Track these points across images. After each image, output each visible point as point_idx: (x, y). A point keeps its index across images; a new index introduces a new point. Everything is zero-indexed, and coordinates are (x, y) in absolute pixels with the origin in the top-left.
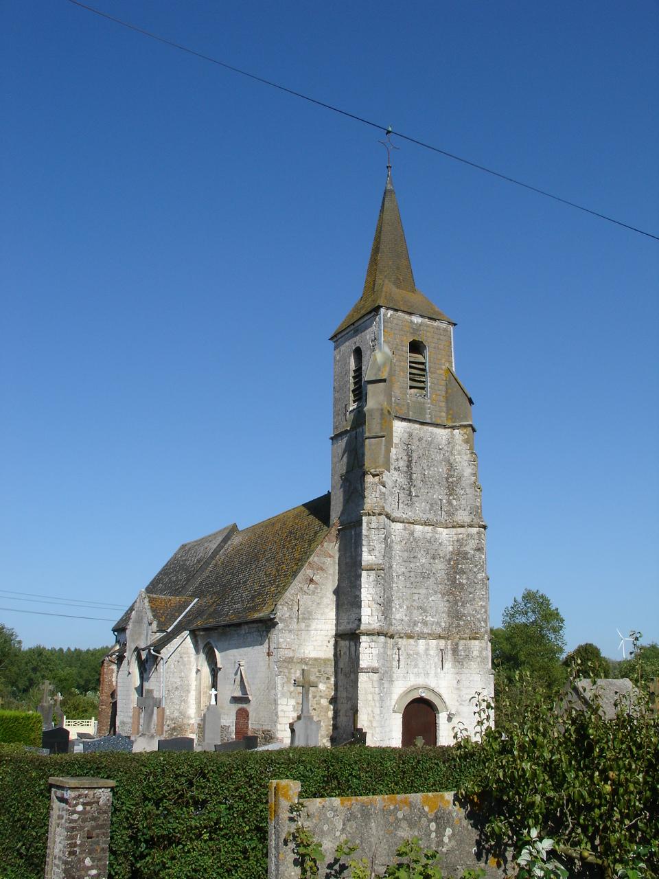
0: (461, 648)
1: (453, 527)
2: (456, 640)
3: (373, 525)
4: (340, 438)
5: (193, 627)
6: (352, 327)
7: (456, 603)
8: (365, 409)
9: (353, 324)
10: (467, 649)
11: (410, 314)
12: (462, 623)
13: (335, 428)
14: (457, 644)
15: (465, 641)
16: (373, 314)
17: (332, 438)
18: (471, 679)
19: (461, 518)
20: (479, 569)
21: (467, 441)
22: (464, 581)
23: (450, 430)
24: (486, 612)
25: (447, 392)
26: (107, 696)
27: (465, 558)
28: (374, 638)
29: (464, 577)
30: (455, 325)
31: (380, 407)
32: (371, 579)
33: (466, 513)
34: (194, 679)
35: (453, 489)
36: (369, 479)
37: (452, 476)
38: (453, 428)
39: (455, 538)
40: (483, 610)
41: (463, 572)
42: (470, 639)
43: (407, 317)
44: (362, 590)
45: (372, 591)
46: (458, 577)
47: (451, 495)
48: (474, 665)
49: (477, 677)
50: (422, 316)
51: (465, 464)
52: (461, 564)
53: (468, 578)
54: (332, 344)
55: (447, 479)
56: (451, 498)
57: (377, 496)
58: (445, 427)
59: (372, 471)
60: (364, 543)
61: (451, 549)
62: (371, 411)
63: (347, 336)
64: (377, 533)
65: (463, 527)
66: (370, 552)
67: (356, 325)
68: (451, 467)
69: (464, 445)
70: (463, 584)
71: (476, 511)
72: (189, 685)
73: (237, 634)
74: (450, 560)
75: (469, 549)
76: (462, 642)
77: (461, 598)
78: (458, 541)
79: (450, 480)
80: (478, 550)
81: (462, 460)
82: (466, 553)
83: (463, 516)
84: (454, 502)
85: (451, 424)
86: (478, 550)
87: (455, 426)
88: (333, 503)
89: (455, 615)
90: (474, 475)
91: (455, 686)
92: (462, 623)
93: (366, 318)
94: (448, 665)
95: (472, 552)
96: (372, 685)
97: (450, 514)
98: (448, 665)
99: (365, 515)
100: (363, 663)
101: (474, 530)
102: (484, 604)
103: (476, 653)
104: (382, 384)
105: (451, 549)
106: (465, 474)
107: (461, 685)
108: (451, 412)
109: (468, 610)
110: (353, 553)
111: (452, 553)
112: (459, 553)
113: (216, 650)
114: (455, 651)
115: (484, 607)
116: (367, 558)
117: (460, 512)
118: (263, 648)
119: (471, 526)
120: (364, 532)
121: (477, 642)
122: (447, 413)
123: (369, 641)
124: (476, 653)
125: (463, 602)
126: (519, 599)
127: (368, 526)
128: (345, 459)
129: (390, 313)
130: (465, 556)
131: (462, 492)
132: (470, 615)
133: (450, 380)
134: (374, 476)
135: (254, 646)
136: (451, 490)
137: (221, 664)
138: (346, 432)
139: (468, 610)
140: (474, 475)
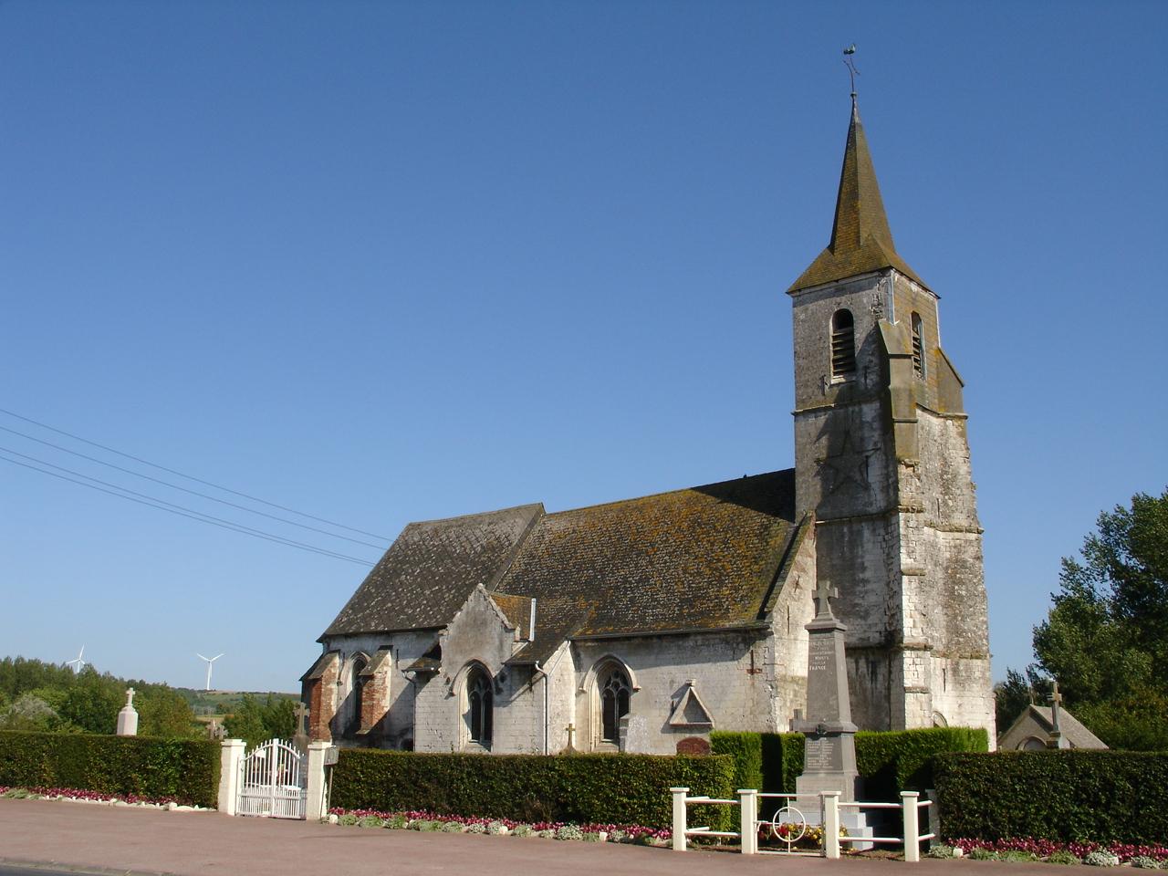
0: (961, 668)
1: (951, 531)
2: (957, 659)
3: (911, 524)
4: (813, 415)
5: (575, 635)
6: (835, 284)
7: (955, 617)
8: (890, 387)
9: (837, 281)
10: (968, 669)
11: (911, 280)
12: (961, 640)
13: (799, 402)
14: (957, 664)
15: (965, 660)
16: (876, 274)
17: (796, 414)
18: (974, 702)
19: (958, 521)
20: (980, 580)
21: (962, 435)
22: (964, 593)
23: (942, 420)
24: (987, 628)
25: (938, 377)
26: (325, 726)
27: (963, 566)
28: (920, 653)
29: (964, 587)
30: (939, 298)
31: (907, 387)
32: (914, 585)
33: (964, 516)
34: (574, 703)
35: (949, 488)
36: (902, 470)
37: (946, 473)
38: (946, 417)
39: (952, 543)
40: (985, 626)
41: (961, 582)
42: (972, 657)
43: (907, 282)
44: (903, 597)
45: (915, 599)
46: (956, 587)
47: (946, 494)
48: (976, 687)
49: (980, 702)
50: (919, 285)
51: (961, 460)
52: (960, 573)
53: (967, 590)
54: (790, 299)
55: (942, 476)
56: (947, 497)
57: (913, 489)
58: (938, 416)
59: (907, 460)
60: (902, 543)
61: (948, 556)
62: (897, 390)
63: (821, 293)
64: (916, 532)
65: (961, 531)
66: (909, 554)
67: (840, 282)
68: (946, 463)
69: (959, 439)
70: (962, 596)
71: (972, 515)
72: (569, 711)
73: (679, 646)
74: (947, 568)
75: (968, 556)
76: (963, 661)
77: (961, 612)
78: (955, 547)
79: (945, 477)
80: (978, 558)
81: (957, 455)
82: (965, 562)
83: (960, 520)
84: (950, 503)
85: (946, 414)
86: (978, 558)
87: (949, 416)
88: (800, 492)
89: (955, 630)
90: (970, 473)
91: (956, 710)
92: (961, 640)
93: (863, 277)
94: (949, 687)
95: (971, 560)
96: (921, 706)
97: (947, 516)
98: (949, 687)
99: (903, 510)
100: (908, 683)
101: (973, 536)
102: (985, 619)
103: (978, 674)
104: (907, 360)
105: (948, 556)
106: (962, 472)
107: (963, 709)
108: (944, 399)
109: (968, 625)
110: (847, 554)
111: (949, 560)
112: (957, 561)
113: (627, 666)
114: (955, 671)
115: (985, 622)
116: (905, 561)
117: (957, 515)
118: (745, 661)
119: (970, 531)
120: (902, 531)
121: (978, 662)
122: (940, 401)
123: (913, 656)
124: (978, 674)
125: (963, 616)
126: (1048, 622)
127: (905, 524)
128: (824, 440)
129: (897, 276)
130: (963, 564)
131: (958, 492)
132: (970, 630)
133: (941, 363)
134: (908, 466)
135: (716, 661)
136: (946, 489)
137: (638, 683)
138: (826, 409)
139: (968, 625)
140: (970, 473)
